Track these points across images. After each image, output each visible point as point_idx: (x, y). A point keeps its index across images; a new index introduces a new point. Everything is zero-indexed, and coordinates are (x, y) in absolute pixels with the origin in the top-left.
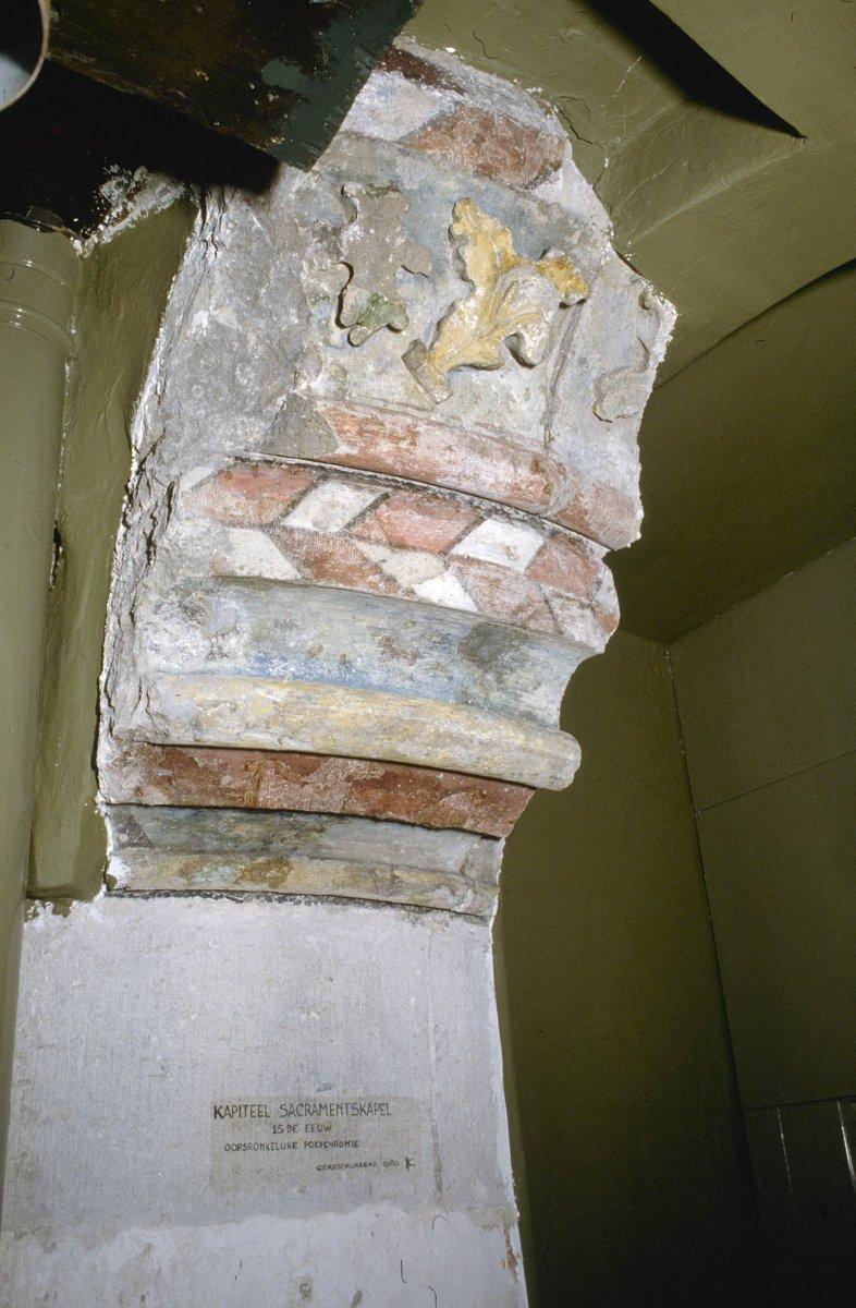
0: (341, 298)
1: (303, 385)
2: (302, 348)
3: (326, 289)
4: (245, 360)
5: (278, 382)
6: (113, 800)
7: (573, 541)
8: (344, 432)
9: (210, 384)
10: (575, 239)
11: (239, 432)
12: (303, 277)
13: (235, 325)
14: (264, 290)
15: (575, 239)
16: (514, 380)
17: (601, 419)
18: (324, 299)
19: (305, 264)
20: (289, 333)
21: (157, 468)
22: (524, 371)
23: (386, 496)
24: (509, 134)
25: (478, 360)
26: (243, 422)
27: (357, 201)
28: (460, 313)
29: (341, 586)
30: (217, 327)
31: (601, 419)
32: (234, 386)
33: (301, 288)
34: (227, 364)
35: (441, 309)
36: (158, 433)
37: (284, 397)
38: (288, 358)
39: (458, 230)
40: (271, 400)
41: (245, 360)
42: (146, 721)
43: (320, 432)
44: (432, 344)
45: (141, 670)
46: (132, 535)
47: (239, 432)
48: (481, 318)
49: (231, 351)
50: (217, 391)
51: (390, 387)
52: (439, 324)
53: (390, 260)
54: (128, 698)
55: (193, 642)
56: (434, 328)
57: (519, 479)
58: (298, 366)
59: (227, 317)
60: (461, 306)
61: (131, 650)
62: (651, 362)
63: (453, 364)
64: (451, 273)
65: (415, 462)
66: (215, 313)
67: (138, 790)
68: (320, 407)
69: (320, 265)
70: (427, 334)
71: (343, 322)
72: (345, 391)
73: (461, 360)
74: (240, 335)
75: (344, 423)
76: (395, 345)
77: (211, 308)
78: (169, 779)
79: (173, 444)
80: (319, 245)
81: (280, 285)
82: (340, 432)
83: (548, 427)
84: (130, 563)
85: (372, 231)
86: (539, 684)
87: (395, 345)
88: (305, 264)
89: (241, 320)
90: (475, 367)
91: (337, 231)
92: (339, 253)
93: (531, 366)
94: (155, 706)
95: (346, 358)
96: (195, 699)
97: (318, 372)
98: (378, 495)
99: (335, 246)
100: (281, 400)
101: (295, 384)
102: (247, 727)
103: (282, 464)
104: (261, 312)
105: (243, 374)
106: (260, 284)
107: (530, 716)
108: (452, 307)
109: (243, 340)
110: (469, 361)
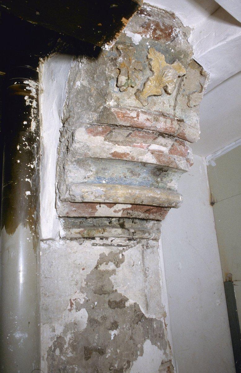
0: (117, 79)
1: (108, 103)
2: (107, 92)
3: (113, 75)
4: (91, 96)
5: (100, 102)
6: (61, 216)
7: (181, 142)
8: (119, 117)
9: (81, 102)
10: (182, 57)
11: (90, 117)
12: (107, 73)
13: (88, 86)
14: (95, 76)
15: (182, 57)
16: (165, 97)
17: (189, 107)
18: (112, 78)
19: (107, 69)
20: (103, 88)
21: (68, 127)
22: (168, 96)
23: (130, 134)
24: (163, 28)
25: (156, 94)
26: (91, 114)
27: (121, 51)
28: (150, 80)
29: (119, 159)
30: (83, 86)
31: (189, 107)
32: (88, 103)
33: (106, 76)
34: (86, 97)
35: (145, 79)
36: (68, 116)
37: (102, 107)
38: (103, 95)
39: (149, 57)
40: (99, 107)
41: (91, 96)
42: (69, 196)
43: (113, 117)
44: (143, 90)
45: (67, 183)
46: (62, 145)
47: (90, 117)
48: (156, 82)
49: (87, 93)
50: (84, 104)
51: (131, 102)
52: (144, 84)
53: (131, 67)
54: (64, 190)
56: (143, 85)
57: (167, 127)
58: (106, 97)
59: (85, 83)
60: (151, 78)
61: (64, 177)
62: (203, 90)
63: (149, 95)
64: (147, 68)
65: (139, 124)
66: (82, 82)
67: (67, 213)
68: (112, 110)
69: (111, 69)
70: (141, 87)
71: (118, 85)
72: (119, 104)
73: (150, 94)
74: (89, 88)
75: (119, 115)
76: (132, 91)
77: (81, 80)
78: (75, 211)
79: (72, 120)
80: (111, 63)
81: (100, 74)
82: (118, 117)
83: (174, 110)
84: (62, 153)
85: (125, 59)
86: (172, 180)
87: (132, 91)
88: (107, 69)
89: (89, 84)
90: (155, 96)
91: (116, 59)
92: (116, 66)
93: (170, 94)
94: (71, 193)
95: (119, 95)
96: (82, 191)
97: (111, 99)
98: (129, 133)
99: (115, 64)
100: (102, 107)
101: (105, 103)
102: (96, 197)
103: (102, 126)
104: (95, 82)
105: (91, 100)
106: (94, 74)
107: (170, 189)
108: (148, 79)
109: (90, 89)
110: (153, 94)
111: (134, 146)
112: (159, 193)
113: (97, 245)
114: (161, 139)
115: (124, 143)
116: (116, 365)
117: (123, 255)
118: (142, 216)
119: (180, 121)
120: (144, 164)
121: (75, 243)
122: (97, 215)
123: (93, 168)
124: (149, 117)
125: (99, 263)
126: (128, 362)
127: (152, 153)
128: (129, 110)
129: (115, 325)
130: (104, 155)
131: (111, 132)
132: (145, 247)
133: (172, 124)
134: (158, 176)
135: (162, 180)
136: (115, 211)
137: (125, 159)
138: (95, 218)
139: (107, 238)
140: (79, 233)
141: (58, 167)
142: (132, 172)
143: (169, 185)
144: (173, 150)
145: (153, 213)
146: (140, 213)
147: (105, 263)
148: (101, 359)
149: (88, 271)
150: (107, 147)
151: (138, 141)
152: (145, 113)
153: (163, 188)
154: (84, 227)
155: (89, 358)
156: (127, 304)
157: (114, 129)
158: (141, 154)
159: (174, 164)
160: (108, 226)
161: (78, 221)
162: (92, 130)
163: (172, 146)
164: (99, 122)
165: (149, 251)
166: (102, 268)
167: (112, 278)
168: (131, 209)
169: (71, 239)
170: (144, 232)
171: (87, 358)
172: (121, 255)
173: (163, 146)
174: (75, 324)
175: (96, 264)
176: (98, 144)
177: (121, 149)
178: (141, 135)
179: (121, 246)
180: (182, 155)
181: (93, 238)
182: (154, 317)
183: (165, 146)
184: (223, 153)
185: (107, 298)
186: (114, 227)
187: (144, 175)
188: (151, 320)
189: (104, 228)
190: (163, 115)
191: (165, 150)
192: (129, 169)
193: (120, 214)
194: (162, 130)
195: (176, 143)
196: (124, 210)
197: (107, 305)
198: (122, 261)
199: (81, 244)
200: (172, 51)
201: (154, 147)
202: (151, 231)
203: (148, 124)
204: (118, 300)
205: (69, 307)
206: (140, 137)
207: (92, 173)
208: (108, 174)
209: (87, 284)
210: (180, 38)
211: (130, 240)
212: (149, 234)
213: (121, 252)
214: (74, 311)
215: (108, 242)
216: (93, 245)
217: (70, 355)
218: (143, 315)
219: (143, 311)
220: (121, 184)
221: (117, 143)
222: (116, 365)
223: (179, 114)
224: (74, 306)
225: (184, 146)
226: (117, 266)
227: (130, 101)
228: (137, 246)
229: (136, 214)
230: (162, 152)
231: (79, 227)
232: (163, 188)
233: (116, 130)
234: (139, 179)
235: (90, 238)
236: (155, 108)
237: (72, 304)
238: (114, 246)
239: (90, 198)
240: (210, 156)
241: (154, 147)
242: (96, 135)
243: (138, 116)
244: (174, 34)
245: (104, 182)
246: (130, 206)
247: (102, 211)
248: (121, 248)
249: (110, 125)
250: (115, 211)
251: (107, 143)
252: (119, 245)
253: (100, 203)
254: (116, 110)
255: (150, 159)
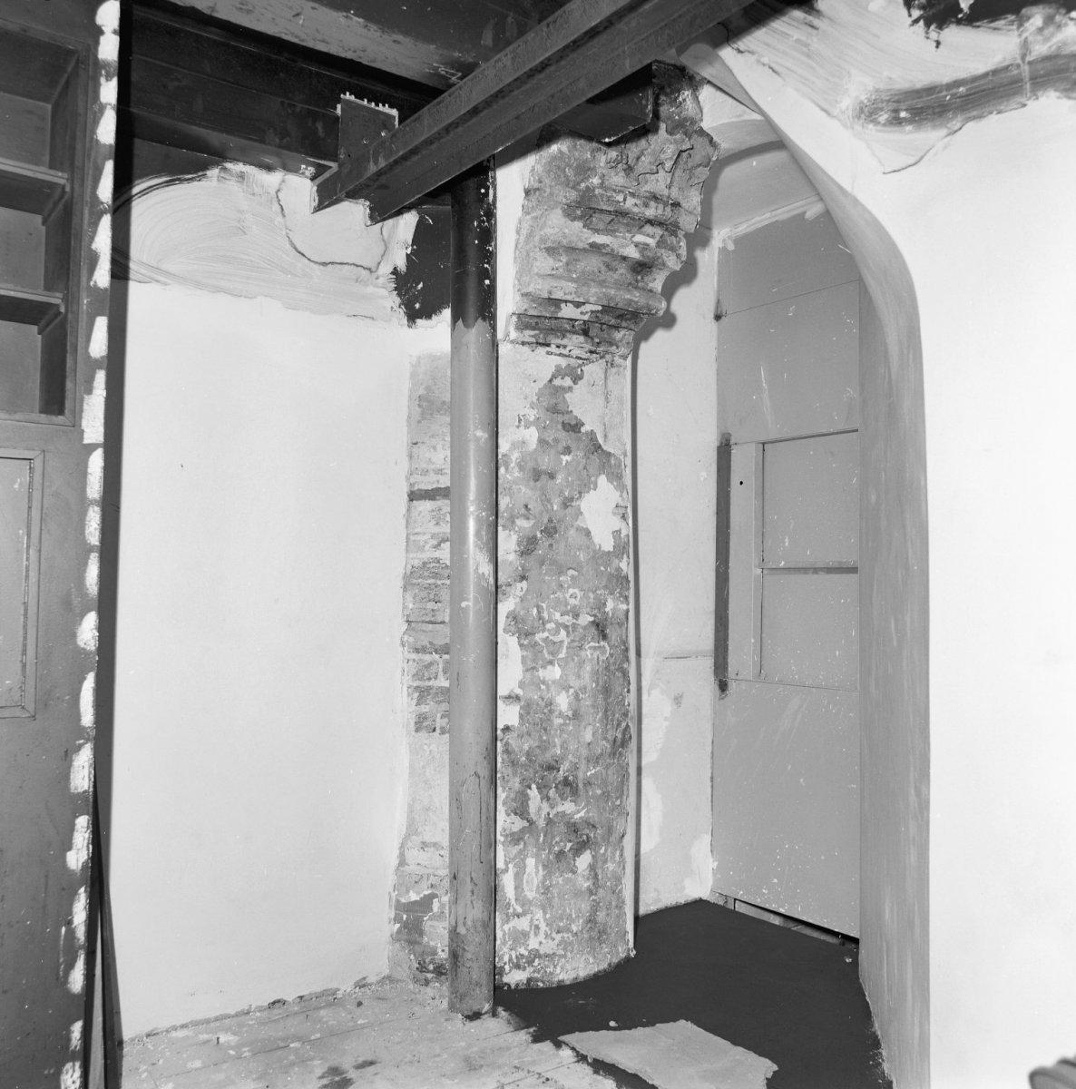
5: (581, 177)
7: (674, 231)
23: (612, 220)
32: (566, 176)
36: (536, 185)
40: (579, 184)
55: (550, 262)
107: (651, 291)
109: (569, 158)
111: (616, 237)
112: (638, 295)
113: (552, 354)
114: (648, 229)
115: (608, 231)
116: (567, 494)
117: (581, 370)
118: (613, 322)
119: (676, 205)
120: (624, 258)
121: (526, 349)
122: (560, 315)
123: (564, 259)
124: (638, 202)
125: (554, 377)
126: (580, 493)
127: (636, 246)
128: (614, 191)
129: (567, 450)
130: (581, 245)
131: (591, 216)
132: (609, 365)
133: (664, 210)
134: (638, 273)
135: (642, 279)
136: (582, 313)
137: (604, 251)
138: (556, 318)
139: (565, 347)
140: (532, 336)
141: (518, 252)
142: (607, 266)
143: (651, 285)
144: (661, 243)
145: (626, 320)
146: (611, 318)
147: (560, 377)
148: (551, 483)
149: (541, 384)
150: (586, 236)
151: (621, 229)
152: (633, 195)
153: (644, 289)
154: (539, 329)
155: (538, 480)
156: (583, 430)
157: (595, 213)
158: (623, 246)
159: (660, 260)
160: (567, 331)
161: (533, 321)
162: (570, 212)
163: (661, 237)
164: (579, 204)
165: (614, 370)
166: (557, 382)
167: (567, 396)
168: (601, 312)
169: (523, 343)
170: (611, 344)
171: (536, 480)
172: (579, 370)
173: (648, 237)
174: (524, 443)
175: (550, 377)
176: (577, 232)
177: (600, 239)
178: (625, 221)
179: (581, 358)
180: (673, 249)
181: (548, 345)
182: (612, 452)
183: (653, 237)
184: (748, 230)
185: (560, 418)
186: (574, 333)
187: (622, 271)
188: (609, 454)
189: (563, 333)
190: (655, 198)
191: (652, 242)
192: (604, 263)
193: (586, 317)
194: (652, 217)
195: (666, 233)
196: (592, 312)
197: (560, 427)
198: (581, 378)
199: (533, 351)
200: (677, 117)
201: (639, 238)
202: (620, 344)
203: (636, 210)
204: (573, 422)
205: (517, 423)
206: (623, 224)
207: (561, 264)
208: (580, 266)
209: (538, 400)
210: (689, 103)
211: (591, 352)
212: (617, 348)
213: (580, 366)
214: (522, 428)
215: (565, 352)
216: (548, 353)
217: (517, 474)
218: (600, 447)
219: (601, 441)
220: (593, 280)
221: (597, 231)
222: (567, 494)
223: (675, 193)
224: (523, 423)
225: (676, 236)
226: (575, 383)
227: (618, 179)
228: (600, 361)
229: (606, 318)
230: (648, 245)
231: (534, 329)
232: (644, 289)
233: (597, 215)
234: (616, 276)
235: (543, 344)
236: (647, 188)
237: (520, 421)
238: (572, 357)
239: (558, 295)
240: (727, 230)
241: (639, 238)
242: (574, 219)
243: (625, 200)
244: (681, 99)
245: (574, 276)
246: (600, 308)
247: (567, 311)
248: (581, 362)
249: (590, 208)
250: (582, 313)
251: (585, 230)
252: (578, 358)
253: (566, 302)
254: (601, 191)
255: (633, 253)
